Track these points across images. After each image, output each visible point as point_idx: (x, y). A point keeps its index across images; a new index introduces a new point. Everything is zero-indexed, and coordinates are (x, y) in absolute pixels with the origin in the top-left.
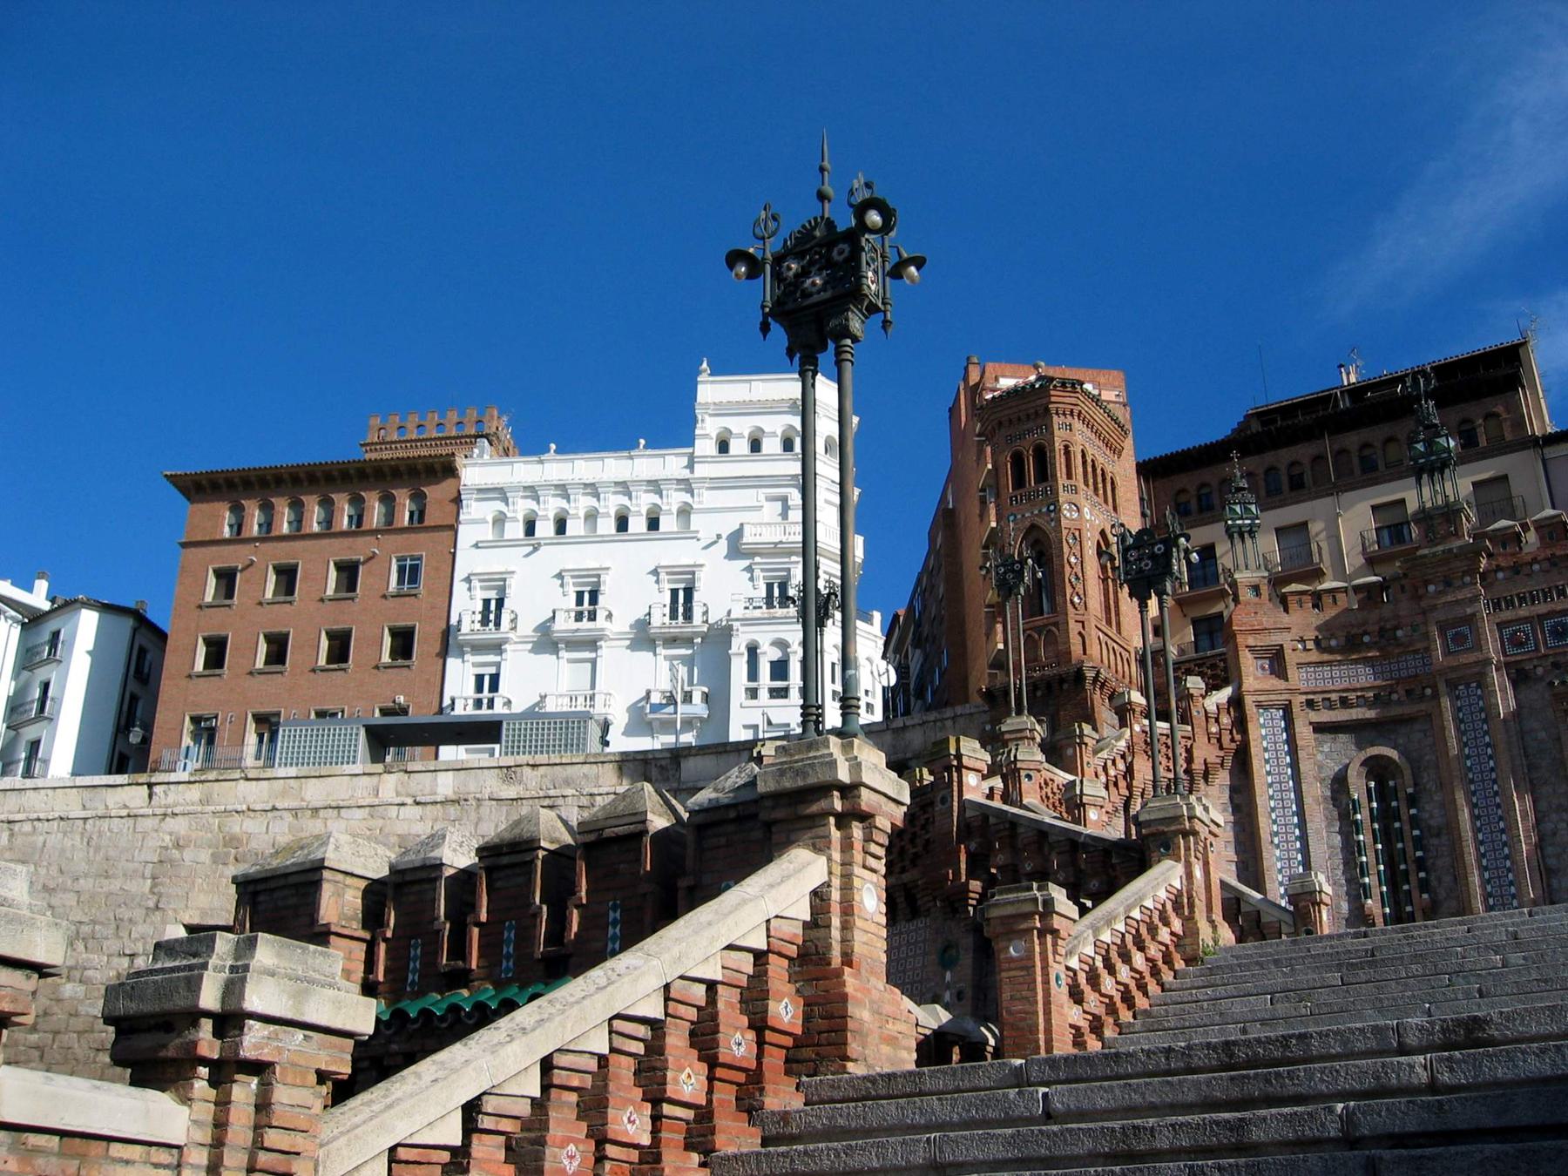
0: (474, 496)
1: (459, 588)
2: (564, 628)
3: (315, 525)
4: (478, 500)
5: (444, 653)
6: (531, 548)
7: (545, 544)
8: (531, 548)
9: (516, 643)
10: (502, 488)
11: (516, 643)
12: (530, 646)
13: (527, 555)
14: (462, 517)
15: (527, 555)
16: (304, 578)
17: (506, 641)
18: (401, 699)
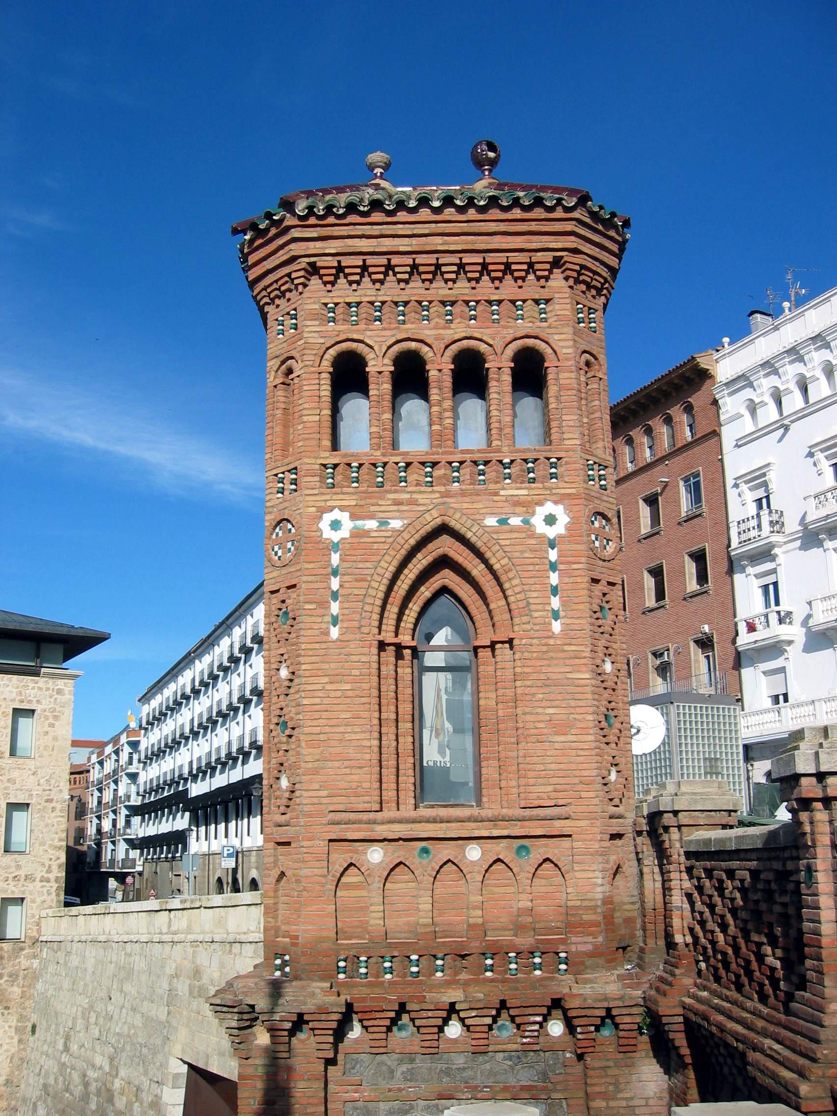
0: (726, 392)
1: (731, 493)
2: (815, 518)
3: (629, 465)
4: (731, 394)
5: (731, 571)
6: (782, 430)
7: (793, 422)
8: (782, 430)
9: (785, 543)
10: (743, 375)
11: (785, 543)
12: (798, 543)
13: (780, 440)
14: (722, 418)
15: (780, 440)
16: (626, 521)
17: (771, 546)
18: (706, 628)
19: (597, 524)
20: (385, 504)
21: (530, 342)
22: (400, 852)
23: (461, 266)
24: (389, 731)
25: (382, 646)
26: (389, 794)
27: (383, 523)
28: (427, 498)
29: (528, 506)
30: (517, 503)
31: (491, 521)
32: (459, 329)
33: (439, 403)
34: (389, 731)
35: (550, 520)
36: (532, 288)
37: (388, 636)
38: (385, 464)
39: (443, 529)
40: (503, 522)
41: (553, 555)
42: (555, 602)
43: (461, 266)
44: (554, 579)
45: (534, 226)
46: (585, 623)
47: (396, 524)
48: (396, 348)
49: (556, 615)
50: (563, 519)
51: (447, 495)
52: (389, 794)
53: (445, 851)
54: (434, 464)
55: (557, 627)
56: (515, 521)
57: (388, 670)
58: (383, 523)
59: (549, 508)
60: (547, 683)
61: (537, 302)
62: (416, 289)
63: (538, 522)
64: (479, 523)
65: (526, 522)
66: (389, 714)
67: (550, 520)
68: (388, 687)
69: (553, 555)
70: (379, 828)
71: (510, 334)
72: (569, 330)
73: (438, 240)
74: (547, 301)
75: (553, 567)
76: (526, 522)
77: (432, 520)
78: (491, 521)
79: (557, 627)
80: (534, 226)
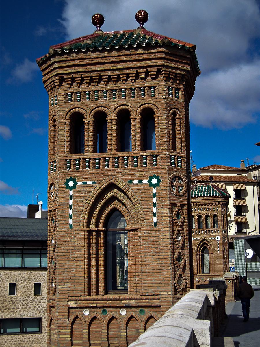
19: (224, 238)
20: (197, 236)
21: (215, 214)
22: (200, 279)
23: (206, 204)
24: (198, 264)
25: (197, 254)
26: (199, 272)
27: (197, 239)
28: (202, 235)
29: (215, 236)
30: (213, 236)
31: (210, 238)
32: (206, 212)
33: (204, 222)
34: (198, 264)
35: (218, 238)
36: (216, 206)
37: (198, 253)
38: (197, 231)
39: (204, 239)
40: (212, 238)
41: (218, 243)
42: (218, 249)
43: (206, 204)
44: (218, 246)
45: (216, 198)
46: (222, 251)
47: (198, 239)
48: (198, 215)
49: (218, 250)
50: (219, 238)
51: (205, 235)
52: (199, 272)
53: (205, 279)
54: (203, 231)
55: (218, 252)
56: (213, 238)
57: (198, 257)
58: (197, 239)
59: (218, 236)
60: (217, 259)
61: (216, 208)
62: (201, 207)
63: (216, 238)
64: (209, 238)
65: (215, 238)
66: (198, 262)
67: (218, 238)
68: (198, 259)
69: (218, 243)
70: (197, 276)
71: (213, 213)
72: (221, 212)
73: (203, 200)
74: (218, 208)
75: (218, 244)
76: (215, 238)
77: (203, 238)
78: (210, 238)
79: (218, 252)
80: (216, 198)
